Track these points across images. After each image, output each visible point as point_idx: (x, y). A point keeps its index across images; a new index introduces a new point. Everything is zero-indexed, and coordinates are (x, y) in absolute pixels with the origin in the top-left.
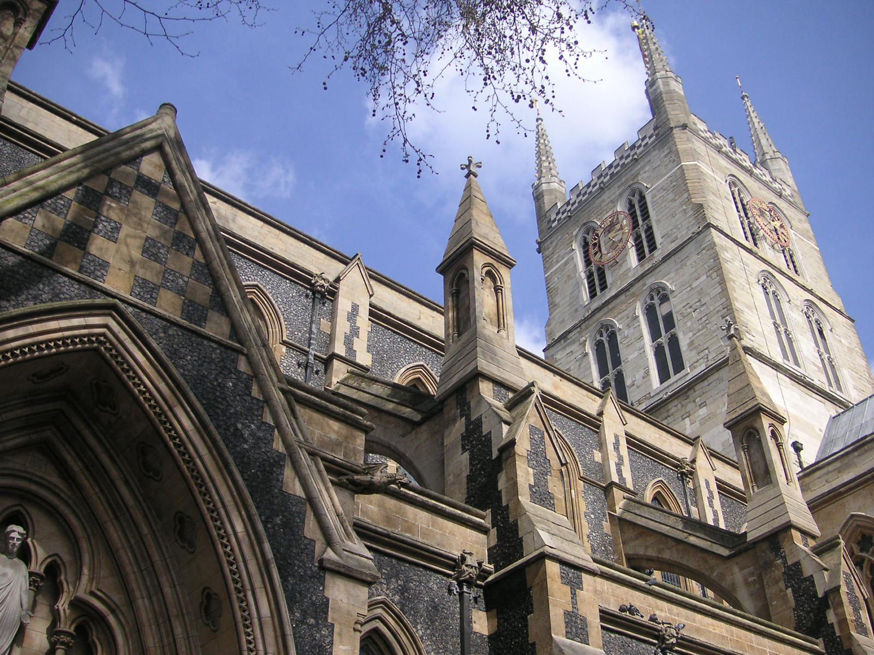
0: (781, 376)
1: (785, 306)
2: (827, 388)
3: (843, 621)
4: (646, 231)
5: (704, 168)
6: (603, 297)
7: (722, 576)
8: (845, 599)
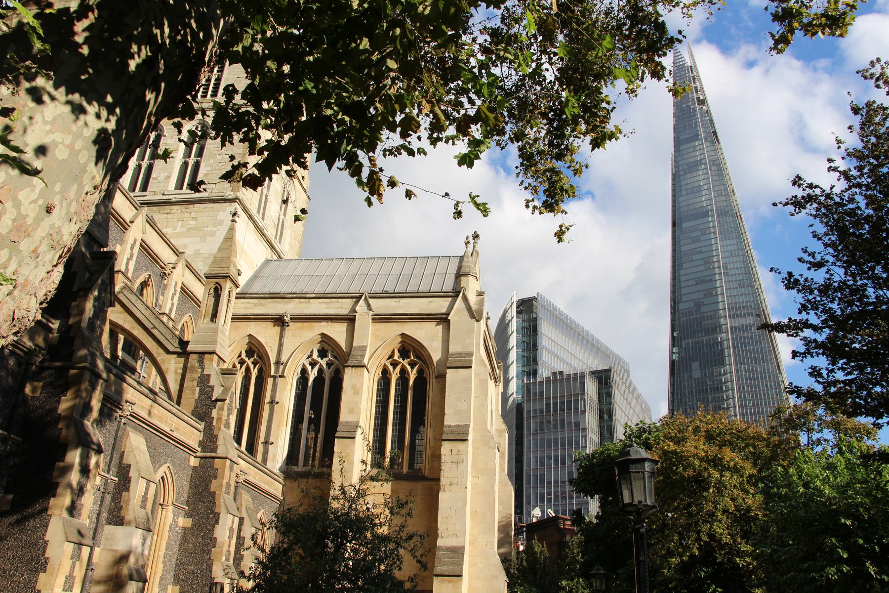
3: (219, 419)
4: (216, 80)
7: (164, 361)
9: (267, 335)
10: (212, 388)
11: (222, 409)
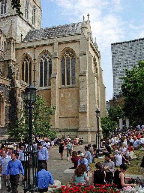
0: (23, 21)
1: (29, 5)
2: (31, 24)
3: (14, 78)
8: (16, 74)
9: (30, 52)
11: (15, 75)
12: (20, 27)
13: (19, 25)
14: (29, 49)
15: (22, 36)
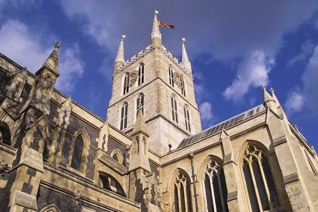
1: (178, 105)
2: (185, 130)
5: (161, 61)
6: (127, 94)
7: (120, 180)
9: (185, 166)
10: (142, 184)
11: (147, 193)
12: (166, 135)
13: (164, 130)
14: (182, 161)
15: (170, 146)
